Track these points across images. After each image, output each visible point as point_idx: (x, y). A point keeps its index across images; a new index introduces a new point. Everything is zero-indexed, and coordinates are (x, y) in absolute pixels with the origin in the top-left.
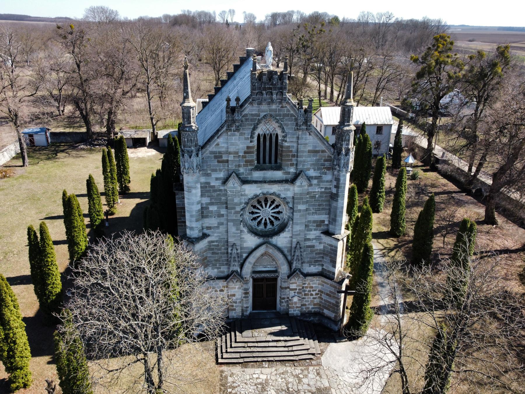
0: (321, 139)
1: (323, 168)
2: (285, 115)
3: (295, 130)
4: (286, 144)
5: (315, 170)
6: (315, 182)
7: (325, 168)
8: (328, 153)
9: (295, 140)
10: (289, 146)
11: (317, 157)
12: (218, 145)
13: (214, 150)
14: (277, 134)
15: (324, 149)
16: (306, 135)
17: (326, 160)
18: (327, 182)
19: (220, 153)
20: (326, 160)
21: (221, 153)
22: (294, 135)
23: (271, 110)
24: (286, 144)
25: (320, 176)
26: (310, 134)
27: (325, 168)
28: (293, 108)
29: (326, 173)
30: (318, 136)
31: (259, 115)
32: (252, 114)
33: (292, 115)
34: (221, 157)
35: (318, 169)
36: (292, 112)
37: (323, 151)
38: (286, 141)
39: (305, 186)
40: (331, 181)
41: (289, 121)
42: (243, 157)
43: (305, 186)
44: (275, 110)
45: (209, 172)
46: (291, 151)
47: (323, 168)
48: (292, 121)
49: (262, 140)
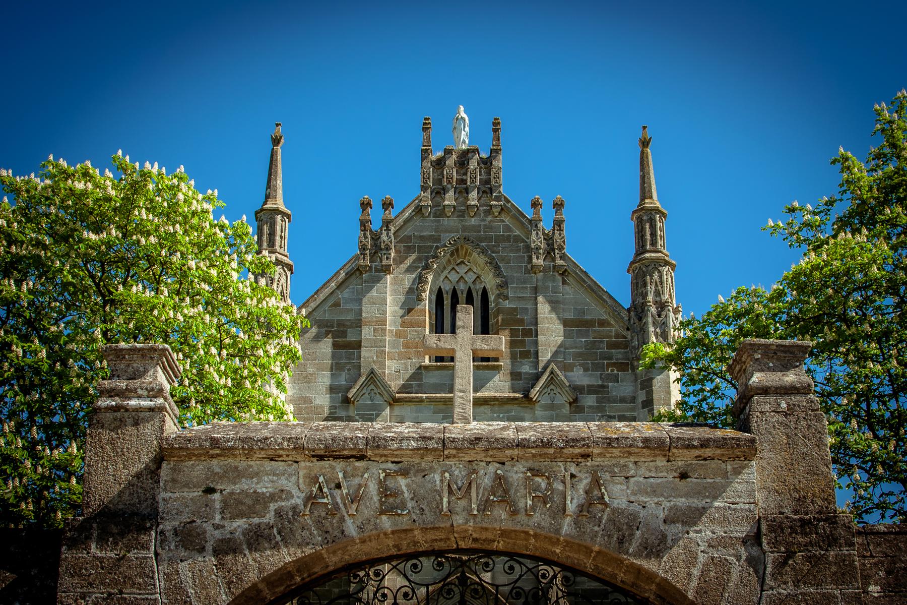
0: (592, 290)
1: (609, 365)
2: (499, 239)
3: (527, 271)
4: (507, 304)
5: (586, 370)
6: (590, 400)
7: (614, 364)
8: (615, 328)
9: (528, 294)
10: (515, 309)
11: (588, 336)
12: (337, 304)
13: (327, 317)
14: (485, 293)
15: (605, 317)
16: (554, 281)
17: (612, 345)
18: (623, 400)
19: (341, 323)
20: (612, 345)
21: (344, 326)
22: (525, 282)
23: (465, 228)
24: (507, 304)
25: (603, 387)
26: (564, 282)
27: (614, 364)
28: (518, 219)
29: (616, 376)
30: (584, 281)
31: (438, 239)
32: (421, 237)
33: (517, 239)
34: (344, 334)
35: (596, 367)
36: (518, 233)
37: (602, 323)
38: (506, 298)
39: (561, 406)
40: (633, 399)
41: (511, 251)
42: (398, 335)
43: (561, 406)
44: (477, 229)
45: (311, 370)
46: (521, 322)
47: (609, 365)
48: (518, 250)
49: (447, 302)
